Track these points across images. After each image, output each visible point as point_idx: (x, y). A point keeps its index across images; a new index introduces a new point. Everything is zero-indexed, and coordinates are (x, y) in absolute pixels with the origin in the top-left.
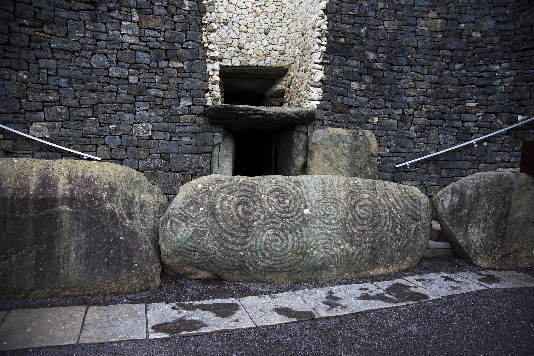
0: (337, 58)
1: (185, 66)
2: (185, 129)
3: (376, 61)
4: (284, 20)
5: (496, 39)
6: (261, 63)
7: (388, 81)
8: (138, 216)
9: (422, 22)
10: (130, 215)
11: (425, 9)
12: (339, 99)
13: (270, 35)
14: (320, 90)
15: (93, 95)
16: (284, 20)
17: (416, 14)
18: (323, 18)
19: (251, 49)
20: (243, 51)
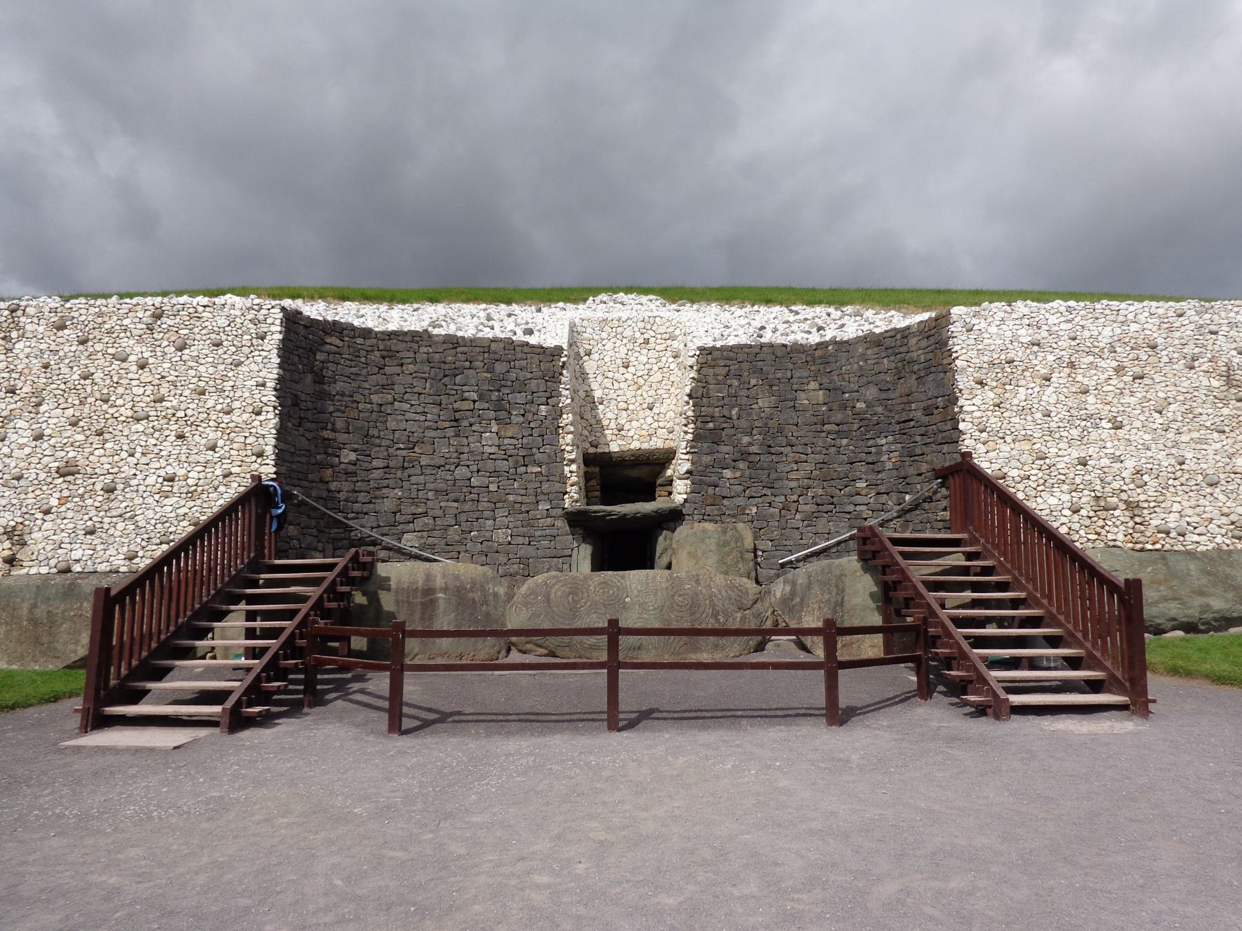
0: (705, 445)
1: (544, 470)
2: (544, 533)
3: (751, 444)
4: (673, 390)
5: (880, 409)
6: (645, 446)
7: (765, 465)
8: (492, 603)
9: (802, 395)
10: (486, 602)
11: (805, 380)
12: (711, 490)
13: (656, 410)
14: (688, 482)
15: (456, 505)
16: (673, 390)
17: (795, 387)
18: (688, 403)
19: (632, 429)
20: (623, 433)
